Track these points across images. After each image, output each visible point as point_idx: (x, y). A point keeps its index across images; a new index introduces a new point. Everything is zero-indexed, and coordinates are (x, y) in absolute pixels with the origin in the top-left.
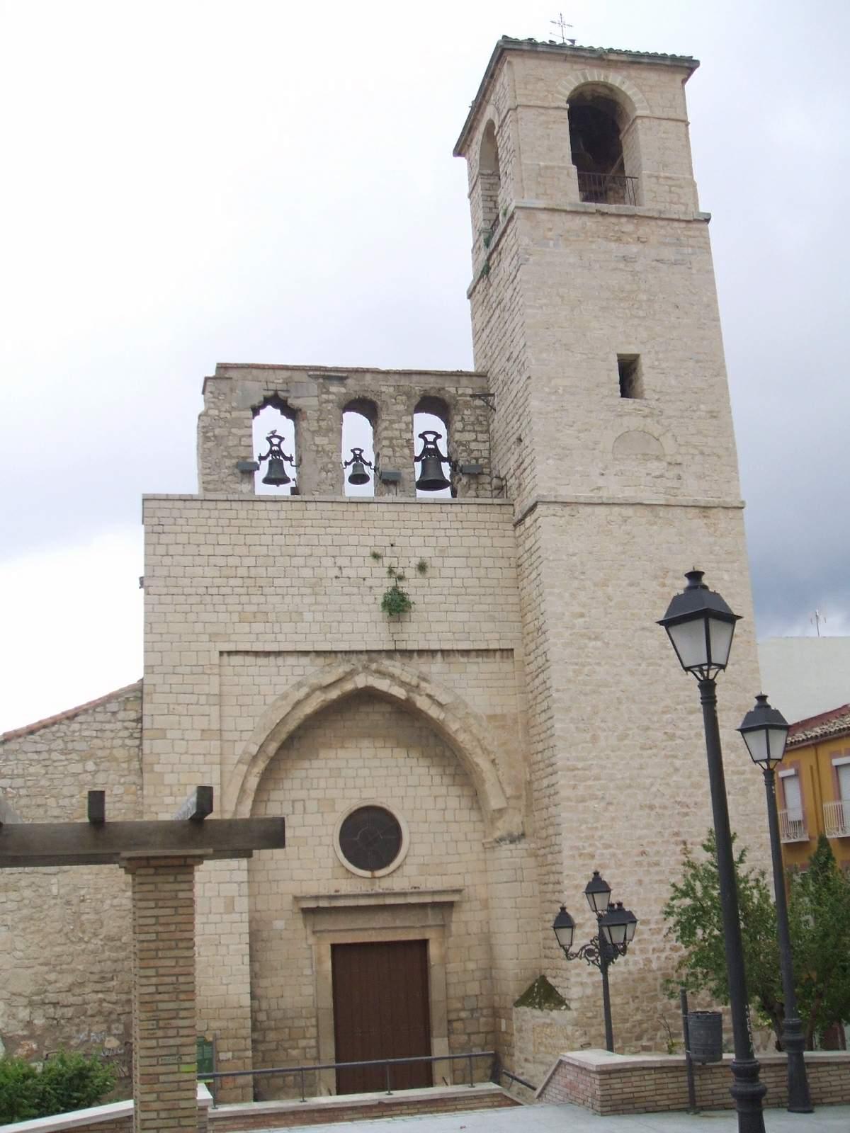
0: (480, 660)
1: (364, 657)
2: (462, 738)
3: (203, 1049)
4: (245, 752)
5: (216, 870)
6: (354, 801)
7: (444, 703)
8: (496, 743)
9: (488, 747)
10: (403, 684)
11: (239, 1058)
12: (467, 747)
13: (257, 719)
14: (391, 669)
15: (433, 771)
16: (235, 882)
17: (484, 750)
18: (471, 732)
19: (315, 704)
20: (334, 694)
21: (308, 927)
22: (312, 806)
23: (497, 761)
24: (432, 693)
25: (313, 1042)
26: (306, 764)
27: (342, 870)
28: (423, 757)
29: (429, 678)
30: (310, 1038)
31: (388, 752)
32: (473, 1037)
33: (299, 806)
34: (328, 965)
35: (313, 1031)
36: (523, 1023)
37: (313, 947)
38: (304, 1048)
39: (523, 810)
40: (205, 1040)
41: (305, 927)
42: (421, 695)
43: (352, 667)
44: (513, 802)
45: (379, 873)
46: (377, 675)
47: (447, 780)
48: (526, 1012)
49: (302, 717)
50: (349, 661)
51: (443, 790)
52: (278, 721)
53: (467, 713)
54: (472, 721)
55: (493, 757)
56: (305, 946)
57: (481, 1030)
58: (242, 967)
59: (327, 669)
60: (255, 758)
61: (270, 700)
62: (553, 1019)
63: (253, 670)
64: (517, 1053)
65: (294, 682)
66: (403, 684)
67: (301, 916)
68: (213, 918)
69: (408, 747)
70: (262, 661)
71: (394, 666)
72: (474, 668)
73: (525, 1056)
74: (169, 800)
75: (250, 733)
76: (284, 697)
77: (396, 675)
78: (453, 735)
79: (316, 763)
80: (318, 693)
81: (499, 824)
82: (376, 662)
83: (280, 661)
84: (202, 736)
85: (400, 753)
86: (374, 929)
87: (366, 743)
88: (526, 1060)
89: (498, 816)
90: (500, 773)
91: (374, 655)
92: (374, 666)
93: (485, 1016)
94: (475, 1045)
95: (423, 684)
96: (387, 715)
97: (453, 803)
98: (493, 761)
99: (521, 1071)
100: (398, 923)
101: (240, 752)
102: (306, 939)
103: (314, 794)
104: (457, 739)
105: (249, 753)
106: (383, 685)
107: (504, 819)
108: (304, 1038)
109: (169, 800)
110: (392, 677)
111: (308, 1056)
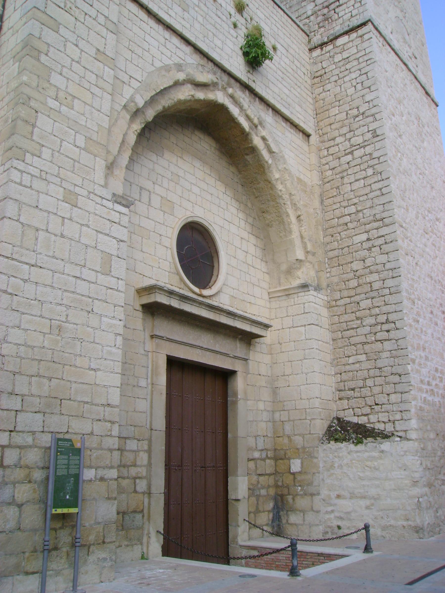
0: (292, 131)
1: (226, 78)
2: (280, 187)
3: (69, 460)
4: (132, 100)
5: (96, 215)
6: (189, 214)
7: (274, 150)
8: (302, 203)
9: (297, 204)
10: (248, 118)
11: (102, 479)
12: (284, 196)
13: (145, 75)
14: (241, 100)
15: (241, 215)
16: (115, 238)
17: (294, 205)
18: (286, 184)
19: (187, 94)
20: (201, 95)
21: (146, 330)
22: (156, 201)
23: (302, 217)
24: (267, 137)
25: (143, 472)
26: (154, 157)
27: (177, 277)
28: (234, 199)
29: (264, 124)
30: (141, 466)
31: (211, 181)
32: (261, 478)
33: (145, 195)
34: (163, 379)
35: (143, 458)
36: (336, 460)
37: (150, 354)
38: (135, 478)
39: (316, 267)
40: (72, 445)
41: (144, 330)
42: (257, 136)
43: (215, 80)
44: (310, 257)
45: (206, 292)
46: (231, 99)
47: (248, 228)
48: (341, 448)
49: (176, 100)
50: (215, 74)
51: (245, 235)
52: (162, 88)
53: (285, 168)
54: (287, 176)
55: (299, 213)
56: (143, 352)
57: (267, 472)
58: (114, 350)
59: (200, 68)
60: (137, 113)
61: (158, 64)
62: (382, 452)
63: (144, 26)
64: (324, 492)
65: (176, 62)
66: (248, 118)
67: (140, 315)
68: (86, 274)
69: (227, 185)
70: (152, 23)
71: (243, 99)
72: (289, 135)
73: (336, 493)
74: (52, 103)
75: (139, 84)
76: (167, 68)
77: (244, 108)
78: (274, 182)
79: (162, 161)
80: (189, 86)
81: (299, 273)
82: (232, 88)
83: (167, 34)
84: (96, 54)
85: (221, 187)
86: (201, 348)
87: (198, 164)
88: (338, 496)
89: (298, 266)
90: (302, 228)
91: (232, 81)
92: (230, 91)
93: (269, 458)
94: (263, 488)
95: (259, 127)
96: (213, 149)
97: (252, 250)
98: (299, 216)
99: (330, 509)
100: (217, 349)
101: (128, 97)
102: (144, 343)
103: (158, 189)
104: (277, 187)
105: (136, 104)
106: (235, 111)
107: (301, 270)
108: (135, 465)
109: (52, 103)
110: (241, 108)
111: (138, 489)
